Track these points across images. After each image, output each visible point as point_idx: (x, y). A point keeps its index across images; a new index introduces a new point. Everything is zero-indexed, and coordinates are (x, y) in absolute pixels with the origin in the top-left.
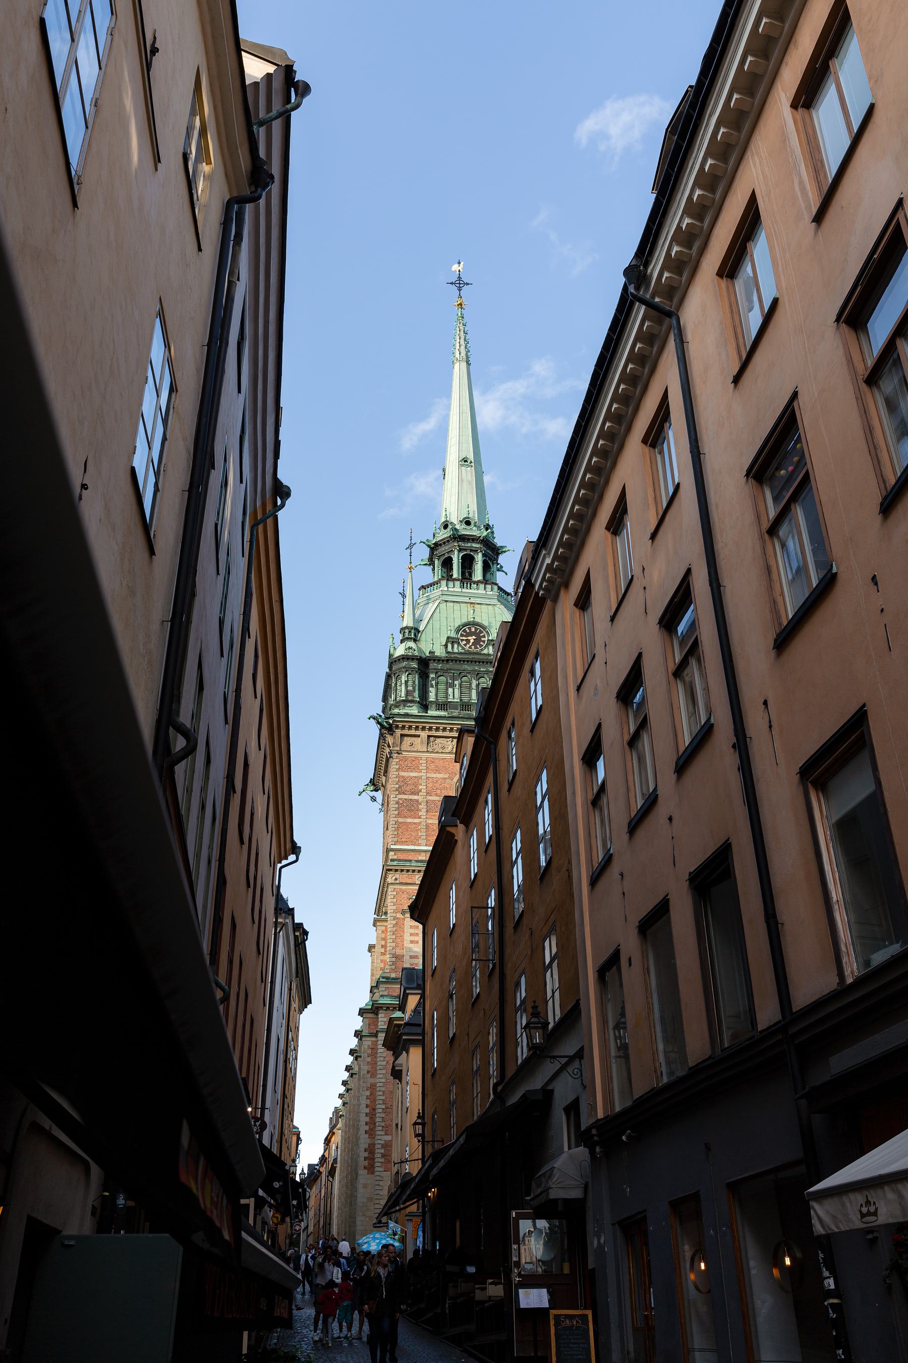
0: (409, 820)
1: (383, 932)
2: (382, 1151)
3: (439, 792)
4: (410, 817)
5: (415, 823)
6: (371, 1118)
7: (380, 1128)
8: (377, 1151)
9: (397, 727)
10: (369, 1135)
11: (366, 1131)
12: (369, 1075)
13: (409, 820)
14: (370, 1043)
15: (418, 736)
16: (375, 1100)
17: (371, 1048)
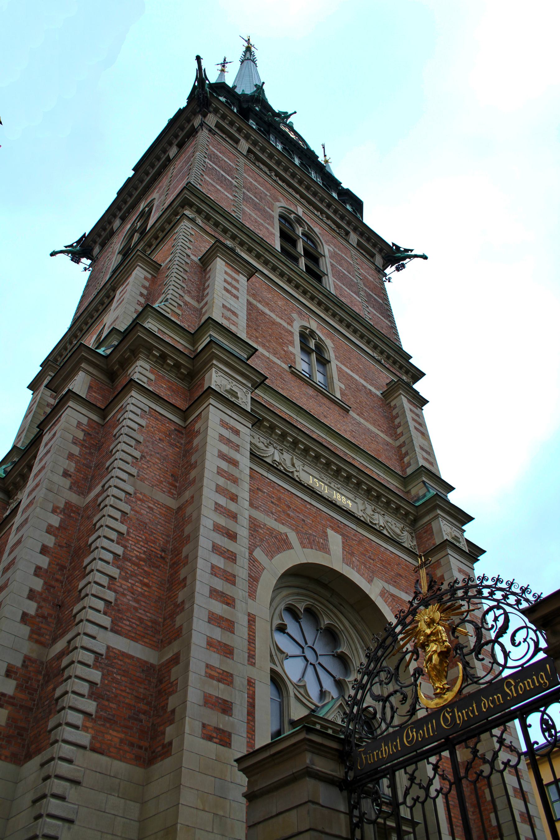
1: (146, 278)
2: (96, 676)
4: (221, 187)
5: (226, 196)
6: (48, 586)
9: (216, 111)
10: (32, 631)
12: (67, 482)
14: (85, 421)
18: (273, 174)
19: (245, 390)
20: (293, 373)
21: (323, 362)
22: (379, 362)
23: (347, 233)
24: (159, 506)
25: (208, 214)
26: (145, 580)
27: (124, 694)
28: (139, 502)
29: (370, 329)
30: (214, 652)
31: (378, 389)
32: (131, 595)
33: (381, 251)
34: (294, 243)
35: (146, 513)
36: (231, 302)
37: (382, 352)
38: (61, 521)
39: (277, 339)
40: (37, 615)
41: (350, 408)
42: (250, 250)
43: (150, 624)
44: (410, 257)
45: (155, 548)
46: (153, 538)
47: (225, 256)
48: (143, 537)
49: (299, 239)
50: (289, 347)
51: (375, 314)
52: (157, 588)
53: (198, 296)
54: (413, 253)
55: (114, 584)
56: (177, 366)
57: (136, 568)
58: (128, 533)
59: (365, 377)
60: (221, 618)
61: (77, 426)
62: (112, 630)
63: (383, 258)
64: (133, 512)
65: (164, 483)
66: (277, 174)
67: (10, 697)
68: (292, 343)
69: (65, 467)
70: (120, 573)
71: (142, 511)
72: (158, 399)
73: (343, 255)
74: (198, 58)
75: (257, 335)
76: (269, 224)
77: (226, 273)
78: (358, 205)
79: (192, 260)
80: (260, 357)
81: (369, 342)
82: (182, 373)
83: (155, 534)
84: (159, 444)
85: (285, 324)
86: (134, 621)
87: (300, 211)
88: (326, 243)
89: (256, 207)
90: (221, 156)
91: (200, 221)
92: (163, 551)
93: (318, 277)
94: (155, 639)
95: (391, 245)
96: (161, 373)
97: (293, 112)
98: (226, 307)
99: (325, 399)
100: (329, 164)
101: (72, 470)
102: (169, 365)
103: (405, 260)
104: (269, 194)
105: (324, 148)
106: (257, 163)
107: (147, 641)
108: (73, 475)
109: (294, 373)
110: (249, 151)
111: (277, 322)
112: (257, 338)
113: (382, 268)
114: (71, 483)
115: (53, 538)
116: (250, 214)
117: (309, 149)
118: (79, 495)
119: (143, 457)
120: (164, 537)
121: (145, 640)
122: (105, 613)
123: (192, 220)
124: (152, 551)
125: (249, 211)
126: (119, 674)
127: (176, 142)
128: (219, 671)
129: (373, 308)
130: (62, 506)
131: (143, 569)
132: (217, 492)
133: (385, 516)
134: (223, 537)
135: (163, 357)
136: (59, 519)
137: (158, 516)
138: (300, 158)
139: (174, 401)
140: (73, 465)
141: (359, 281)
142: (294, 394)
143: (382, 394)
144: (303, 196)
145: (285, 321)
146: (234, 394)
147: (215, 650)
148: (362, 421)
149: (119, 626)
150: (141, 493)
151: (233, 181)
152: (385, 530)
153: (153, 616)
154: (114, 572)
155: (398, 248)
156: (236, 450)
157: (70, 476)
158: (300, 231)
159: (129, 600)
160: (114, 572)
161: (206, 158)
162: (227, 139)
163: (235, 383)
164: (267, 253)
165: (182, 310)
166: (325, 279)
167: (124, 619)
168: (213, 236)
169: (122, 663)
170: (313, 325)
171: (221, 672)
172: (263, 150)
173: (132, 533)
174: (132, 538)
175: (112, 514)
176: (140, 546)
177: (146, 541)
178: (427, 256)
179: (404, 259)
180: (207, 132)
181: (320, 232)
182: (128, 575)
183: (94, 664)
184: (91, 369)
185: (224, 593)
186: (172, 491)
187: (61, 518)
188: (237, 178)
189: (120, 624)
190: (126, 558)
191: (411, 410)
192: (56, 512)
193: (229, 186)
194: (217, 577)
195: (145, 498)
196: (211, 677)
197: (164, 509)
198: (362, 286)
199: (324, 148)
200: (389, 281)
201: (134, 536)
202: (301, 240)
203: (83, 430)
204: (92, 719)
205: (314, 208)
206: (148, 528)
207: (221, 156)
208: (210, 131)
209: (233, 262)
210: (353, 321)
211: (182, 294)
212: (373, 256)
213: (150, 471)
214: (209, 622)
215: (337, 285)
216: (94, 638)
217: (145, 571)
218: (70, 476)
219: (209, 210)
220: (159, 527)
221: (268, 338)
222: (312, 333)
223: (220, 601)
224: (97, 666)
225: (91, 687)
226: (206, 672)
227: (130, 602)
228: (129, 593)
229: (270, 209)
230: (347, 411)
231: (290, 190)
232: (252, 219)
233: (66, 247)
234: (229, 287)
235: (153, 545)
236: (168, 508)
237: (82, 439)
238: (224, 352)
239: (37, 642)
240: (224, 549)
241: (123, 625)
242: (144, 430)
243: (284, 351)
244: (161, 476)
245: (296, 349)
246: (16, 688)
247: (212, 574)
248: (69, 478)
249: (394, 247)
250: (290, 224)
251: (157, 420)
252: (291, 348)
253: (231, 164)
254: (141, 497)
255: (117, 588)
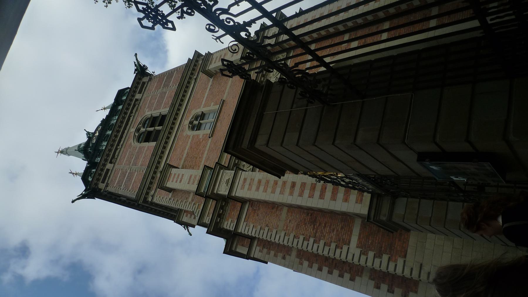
0: (133, 181)
1: (187, 216)
2: (371, 254)
3: (132, 156)
5: (136, 176)
6: (336, 267)
7: (338, 251)
8: (384, 268)
9: (96, 184)
11: (339, 276)
12: (287, 257)
13: (133, 181)
14: (258, 248)
15: (108, 170)
16: (317, 255)
17: (263, 249)
18: (119, 147)
19: (225, 174)
20: (212, 136)
21: (203, 116)
22: (196, 79)
23: (137, 100)
24: (288, 217)
25: (147, 189)
26: (323, 225)
27: (377, 238)
28: (288, 228)
29: (180, 86)
30: (349, 198)
31: (209, 81)
32: (331, 233)
33: (140, 79)
34: (150, 133)
35: (292, 224)
36: (186, 178)
37: (190, 78)
38: (305, 260)
39: (198, 145)
40: (350, 273)
41: (222, 99)
42: (159, 163)
43: (343, 223)
44: (138, 62)
45: (308, 219)
46: (303, 220)
47: (165, 181)
48: (304, 226)
49: (147, 130)
50: (200, 138)
51: (173, 82)
52: (326, 218)
53: (187, 193)
54: (136, 61)
55: (328, 243)
56: (222, 208)
57: (318, 230)
58: (303, 235)
59: (205, 89)
60: (333, 193)
61: (261, 252)
62: (349, 245)
63: (143, 77)
64: (293, 232)
65: (277, 213)
66: (118, 145)
67: (389, 287)
68: (198, 136)
69: (281, 258)
70: (322, 239)
71: (292, 226)
72: (239, 218)
73: (148, 102)
74: (73, 202)
75: (198, 157)
76: (144, 150)
77: (172, 181)
78: (121, 93)
79: (172, 196)
80: (208, 156)
81: (187, 87)
82: (225, 204)
83: (301, 219)
84: (260, 216)
85: (190, 140)
86: (343, 232)
87: (133, 130)
88: (144, 113)
89: (137, 158)
90: (117, 179)
91: (152, 192)
92: (308, 215)
93: (163, 117)
94: (350, 220)
95: (136, 74)
96: (227, 215)
97: (85, 131)
98: (188, 182)
99: (221, 115)
100: (105, 107)
101: (281, 254)
102: (223, 212)
103: (141, 65)
104: (129, 150)
105: (98, 111)
106: (116, 157)
107: (351, 224)
108: (283, 255)
109: (212, 135)
110: (111, 163)
111: (190, 145)
112: (200, 158)
113: (149, 77)
114: (287, 255)
115: (314, 264)
116: (142, 161)
117: (100, 125)
118: (292, 251)
119: (267, 226)
120: (301, 214)
121: (351, 226)
122: (342, 248)
123: (153, 196)
124: (309, 221)
125: (140, 162)
126: (369, 241)
127: (118, 198)
128: (358, 196)
129: (170, 82)
130: (298, 260)
131: (318, 226)
132: (274, 193)
133: (271, 76)
134: (295, 190)
135: (219, 216)
136: (305, 261)
137: (293, 217)
138: (106, 131)
139: (239, 208)
140: (279, 254)
141: (158, 92)
142: (222, 135)
143: (211, 78)
144: (125, 128)
145: (188, 140)
146: (228, 181)
147: (348, 197)
148: (227, 91)
149: (347, 240)
150: (284, 227)
151: (128, 172)
152: (277, 76)
153: (339, 221)
154: (322, 243)
155: (136, 70)
156: (254, 180)
157: (284, 255)
158: (143, 130)
159: (334, 234)
160: (322, 243)
161: (121, 188)
162: (108, 175)
163: (223, 180)
164: (158, 154)
165: (196, 203)
166: (163, 114)
167: (343, 238)
168: (156, 190)
169: (363, 239)
170: (186, 122)
171: (358, 194)
172: (108, 155)
173: (303, 232)
174: (305, 232)
175: (296, 244)
176: (308, 228)
177: (305, 224)
178: (135, 54)
179: (140, 65)
180: (108, 188)
181: (140, 118)
182: (322, 235)
183: (366, 255)
184: (234, 245)
185: (321, 190)
186: (280, 209)
187: (304, 260)
188: (126, 169)
189: (345, 240)
190: (315, 237)
191: (215, 63)
192: (302, 263)
193: (131, 174)
194: (314, 194)
195: (286, 225)
196: (361, 200)
197: (289, 213)
198: (161, 90)
199: (98, 111)
200: (154, 72)
201: (304, 231)
202: (147, 129)
203: (263, 249)
204: (391, 256)
205: (129, 121)
206: (299, 223)
207: (117, 179)
208: (107, 186)
209: (166, 177)
210: (179, 98)
211: (189, 202)
212: (144, 83)
213: (273, 221)
214: (336, 200)
215: (164, 106)
216: (354, 255)
217: (319, 225)
218: (284, 255)
219: (145, 188)
220: (297, 217)
221: (198, 150)
222: (191, 123)
223: (325, 193)
224: (367, 253)
225: (377, 257)
226: (359, 203)
227: (335, 234)
228: (331, 235)
229: (136, 149)
230: (224, 101)
231: (124, 136)
232: (144, 160)
233: (185, 229)
234: (179, 180)
235: (306, 220)
236: (288, 211)
237: (266, 250)
238: (209, 189)
239: (362, 273)
240: (300, 190)
241: (346, 238)
242: (255, 225)
243: (203, 141)
244: (274, 215)
245: (201, 133)
246: (384, 283)
247: (313, 197)
248: (285, 256)
249: (136, 72)
250: (141, 134)
251: (249, 217)
252: (201, 137)
253: (120, 173)
254: (285, 227)
255: (329, 242)
